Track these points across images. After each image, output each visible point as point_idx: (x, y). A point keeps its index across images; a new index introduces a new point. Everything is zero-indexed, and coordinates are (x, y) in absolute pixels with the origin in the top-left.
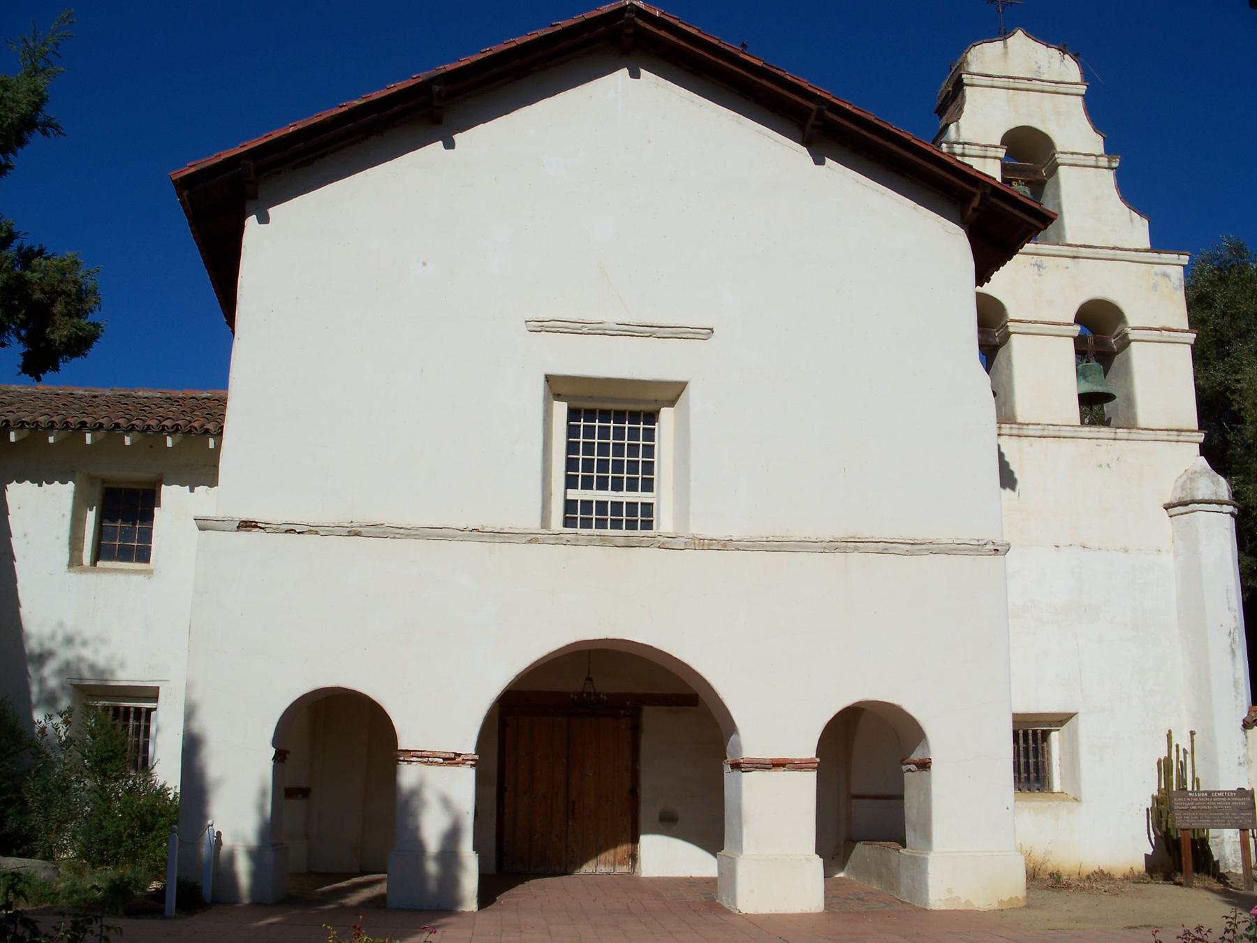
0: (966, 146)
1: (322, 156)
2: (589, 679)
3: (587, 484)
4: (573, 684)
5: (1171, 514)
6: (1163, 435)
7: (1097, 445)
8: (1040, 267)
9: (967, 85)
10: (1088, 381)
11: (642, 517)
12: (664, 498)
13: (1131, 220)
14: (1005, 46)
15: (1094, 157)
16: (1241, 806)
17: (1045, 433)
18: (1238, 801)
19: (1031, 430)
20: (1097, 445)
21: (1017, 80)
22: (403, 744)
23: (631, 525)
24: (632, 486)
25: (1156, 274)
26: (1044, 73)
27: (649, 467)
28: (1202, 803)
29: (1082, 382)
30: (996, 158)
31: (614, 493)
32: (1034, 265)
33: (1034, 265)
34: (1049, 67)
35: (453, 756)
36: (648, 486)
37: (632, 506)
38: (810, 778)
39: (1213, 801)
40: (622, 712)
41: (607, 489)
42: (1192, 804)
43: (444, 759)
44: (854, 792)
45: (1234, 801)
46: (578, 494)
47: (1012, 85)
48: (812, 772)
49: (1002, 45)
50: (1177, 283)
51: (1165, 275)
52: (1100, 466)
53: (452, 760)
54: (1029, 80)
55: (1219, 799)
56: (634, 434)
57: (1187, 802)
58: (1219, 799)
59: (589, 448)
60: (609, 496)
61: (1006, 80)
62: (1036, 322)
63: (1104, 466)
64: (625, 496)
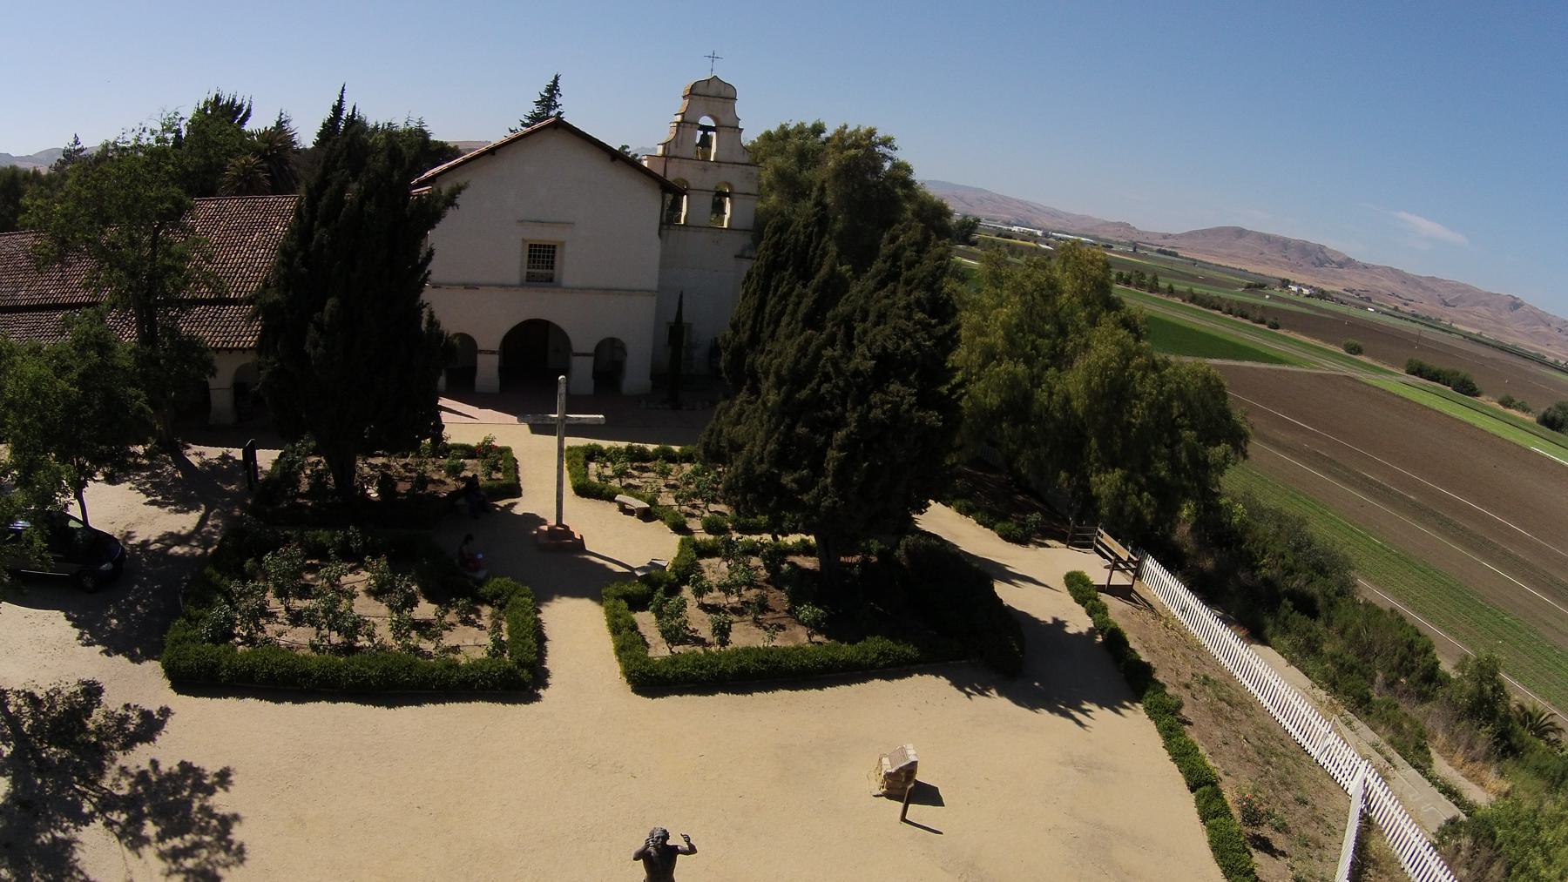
3: (534, 268)
11: (551, 280)
12: (556, 271)
22: (479, 348)
27: (552, 262)
36: (552, 268)
56: (549, 252)
59: (535, 256)
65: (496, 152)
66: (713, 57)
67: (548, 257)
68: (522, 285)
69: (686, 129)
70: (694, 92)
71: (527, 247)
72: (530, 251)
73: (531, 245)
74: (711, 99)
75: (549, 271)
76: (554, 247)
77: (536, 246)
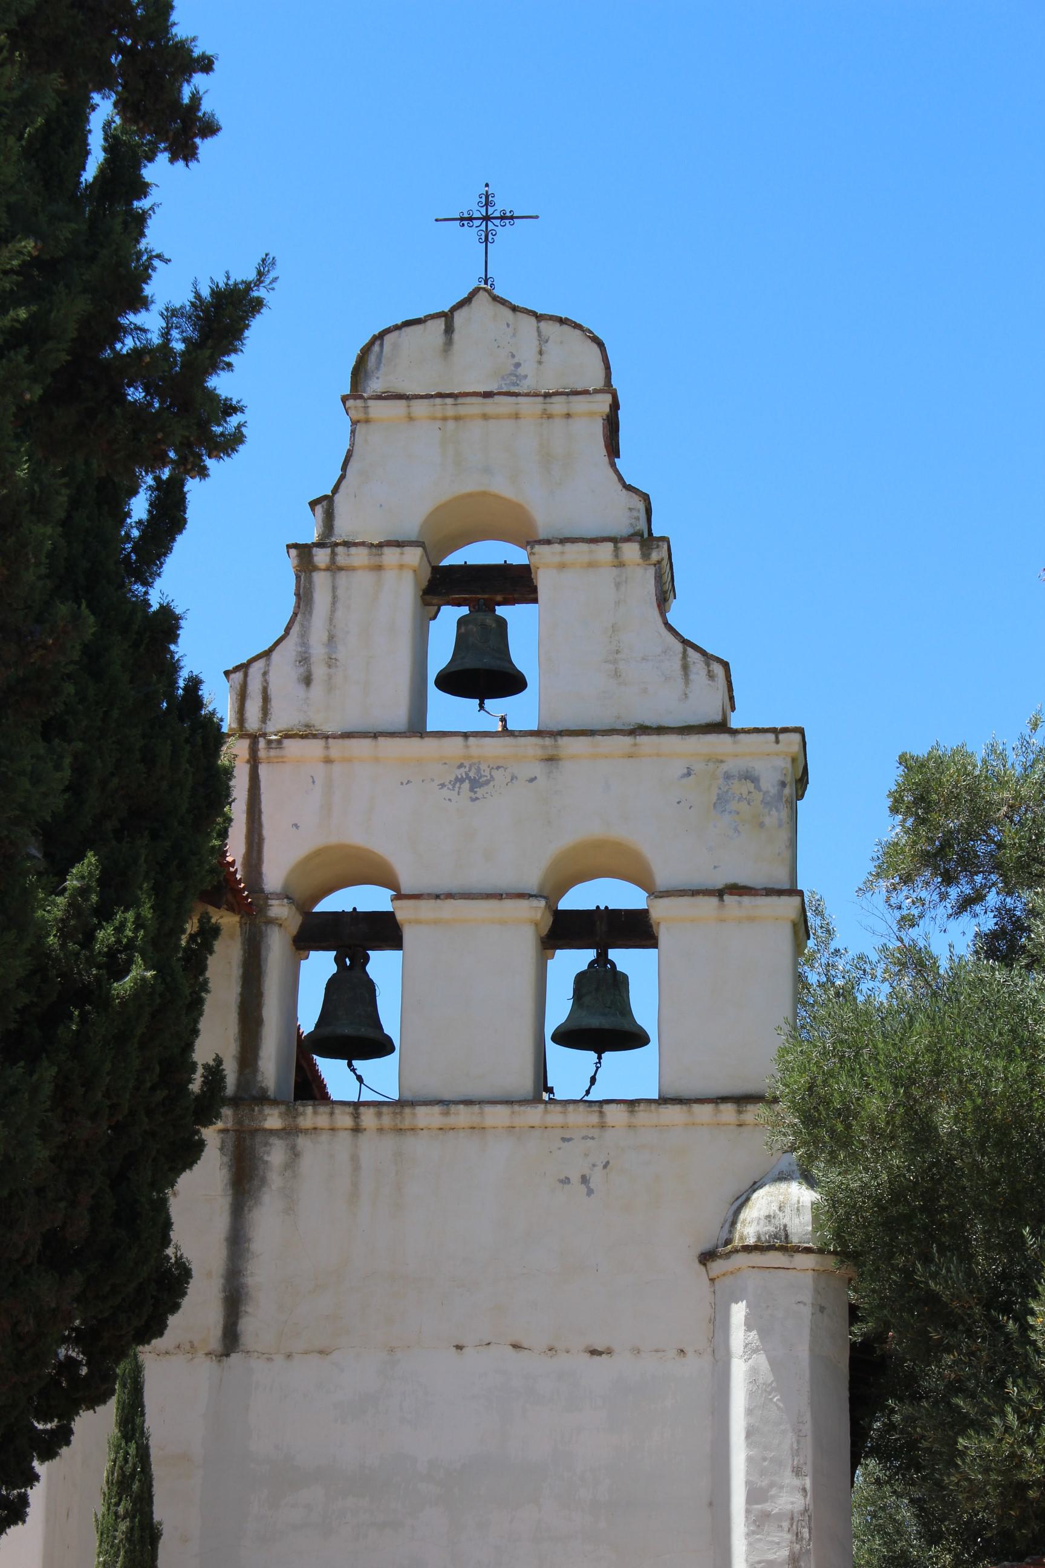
0: (340, 550)
5: (713, 1275)
6: (704, 1112)
7: (564, 1140)
13: (685, 667)
14: (449, 330)
15: (610, 546)
17: (451, 1121)
20: (564, 1140)
21: (460, 400)
25: (728, 776)
26: (526, 377)
30: (401, 567)
32: (461, 780)
33: (461, 780)
34: (540, 363)
47: (450, 411)
49: (443, 327)
50: (774, 791)
51: (749, 777)
52: (566, 1181)
54: (488, 395)
61: (438, 401)
62: (450, 896)
63: (575, 1179)
69: (342, 578)
70: (375, 385)
74: (474, 406)
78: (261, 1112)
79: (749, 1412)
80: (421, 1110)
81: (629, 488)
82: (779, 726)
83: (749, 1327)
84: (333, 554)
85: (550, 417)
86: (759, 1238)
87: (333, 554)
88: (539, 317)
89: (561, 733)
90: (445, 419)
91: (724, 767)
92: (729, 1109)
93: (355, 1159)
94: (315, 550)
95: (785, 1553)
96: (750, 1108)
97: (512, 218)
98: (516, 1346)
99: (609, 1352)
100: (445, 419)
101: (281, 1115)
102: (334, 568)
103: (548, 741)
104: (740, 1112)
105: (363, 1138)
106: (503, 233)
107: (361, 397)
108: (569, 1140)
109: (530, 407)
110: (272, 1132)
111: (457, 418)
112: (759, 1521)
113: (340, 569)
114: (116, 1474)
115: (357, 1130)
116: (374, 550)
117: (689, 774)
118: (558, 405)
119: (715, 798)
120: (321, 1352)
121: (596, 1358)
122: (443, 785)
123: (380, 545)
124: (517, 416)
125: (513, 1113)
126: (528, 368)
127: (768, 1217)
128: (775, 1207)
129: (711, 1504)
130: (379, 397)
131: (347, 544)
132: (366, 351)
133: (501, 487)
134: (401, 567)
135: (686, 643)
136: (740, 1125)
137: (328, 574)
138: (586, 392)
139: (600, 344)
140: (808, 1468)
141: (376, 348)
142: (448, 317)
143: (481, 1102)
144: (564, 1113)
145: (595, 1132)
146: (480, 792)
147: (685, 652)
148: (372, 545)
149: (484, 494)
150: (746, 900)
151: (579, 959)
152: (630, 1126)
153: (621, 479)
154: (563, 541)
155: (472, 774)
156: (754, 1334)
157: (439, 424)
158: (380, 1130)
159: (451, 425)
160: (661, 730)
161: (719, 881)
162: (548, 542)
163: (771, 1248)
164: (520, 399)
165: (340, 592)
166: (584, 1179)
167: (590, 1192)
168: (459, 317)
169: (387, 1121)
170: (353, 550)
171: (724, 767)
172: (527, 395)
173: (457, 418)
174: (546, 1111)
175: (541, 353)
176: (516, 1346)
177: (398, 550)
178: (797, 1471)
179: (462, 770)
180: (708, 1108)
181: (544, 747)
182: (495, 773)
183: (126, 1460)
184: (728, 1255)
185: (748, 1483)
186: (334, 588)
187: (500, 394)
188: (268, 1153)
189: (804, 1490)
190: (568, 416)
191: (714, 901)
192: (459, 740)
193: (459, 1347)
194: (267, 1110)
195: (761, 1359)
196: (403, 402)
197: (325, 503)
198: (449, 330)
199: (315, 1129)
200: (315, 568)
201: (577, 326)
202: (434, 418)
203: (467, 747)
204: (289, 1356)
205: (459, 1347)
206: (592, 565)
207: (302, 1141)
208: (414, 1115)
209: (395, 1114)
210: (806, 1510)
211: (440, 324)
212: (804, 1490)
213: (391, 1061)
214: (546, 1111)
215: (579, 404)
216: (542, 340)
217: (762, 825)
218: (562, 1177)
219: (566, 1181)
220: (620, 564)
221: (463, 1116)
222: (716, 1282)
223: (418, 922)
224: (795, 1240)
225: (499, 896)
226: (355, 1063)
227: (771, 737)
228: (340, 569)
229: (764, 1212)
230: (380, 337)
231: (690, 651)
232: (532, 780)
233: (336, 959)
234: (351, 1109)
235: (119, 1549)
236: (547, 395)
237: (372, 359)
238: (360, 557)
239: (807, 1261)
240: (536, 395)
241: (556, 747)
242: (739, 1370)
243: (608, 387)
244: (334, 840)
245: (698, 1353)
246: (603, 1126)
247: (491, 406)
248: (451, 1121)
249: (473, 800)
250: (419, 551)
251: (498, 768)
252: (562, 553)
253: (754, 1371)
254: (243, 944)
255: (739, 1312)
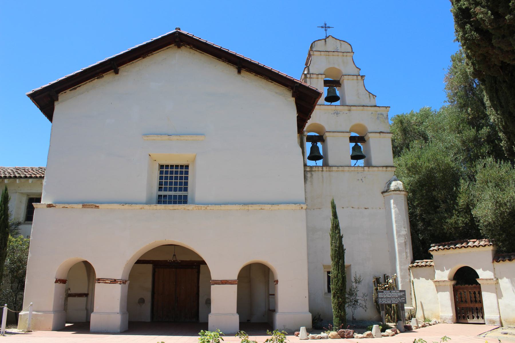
0: (311, 75)
1: (79, 86)
2: (174, 255)
3: (166, 190)
4: (169, 257)
7: (358, 173)
8: (337, 114)
9: (312, 55)
10: (355, 151)
12: (189, 193)
13: (370, 96)
14: (325, 41)
15: (356, 76)
16: (401, 296)
17: (339, 169)
18: (400, 294)
19: (334, 169)
20: (358, 173)
21: (329, 52)
22: (98, 277)
23: (180, 203)
24: (180, 190)
25: (378, 114)
28: (388, 295)
29: (354, 152)
31: (174, 192)
32: (335, 113)
35: (113, 280)
36: (186, 189)
37: (180, 196)
38: (235, 287)
39: (392, 294)
40: (194, 267)
41: (167, 191)
42: (385, 295)
43: (111, 281)
44: (270, 293)
45: (398, 294)
46: (163, 193)
48: (236, 285)
49: (324, 41)
51: (382, 114)
52: (359, 180)
53: (114, 281)
54: (333, 52)
55: (394, 293)
56: (181, 173)
57: (383, 294)
58: (394, 293)
59: (166, 178)
60: (172, 193)
61: (325, 52)
62: (335, 132)
63: (360, 179)
64: (178, 193)
65: (122, 69)
66: (326, 27)
67: (181, 178)
68: (149, 202)
70: (314, 49)
71: (157, 167)
72: (161, 172)
73: (162, 167)
74: (331, 53)
75: (182, 193)
76: (187, 167)
77: (167, 166)
78: (306, 167)
79: (395, 218)
80: (333, 168)
81: (357, 68)
82: (387, 106)
83: (394, 204)
84: (310, 76)
85: (343, 56)
86: (394, 189)
87: (310, 76)
88: (340, 41)
89: (352, 106)
90: (326, 55)
91: (378, 113)
92: (385, 168)
93: (322, 176)
94: (307, 75)
95: (404, 241)
96: (388, 168)
97: (330, 27)
98: (352, 208)
99: (368, 208)
100: (326, 55)
101: (309, 168)
102: (310, 78)
103: (349, 107)
104: (386, 169)
105: (324, 172)
106: (328, 29)
107: (312, 51)
108: (358, 173)
109: (340, 54)
110: (308, 171)
111: (328, 55)
112: (399, 236)
113: (311, 78)
114: (334, 225)
115: (322, 171)
116: (317, 75)
117: (372, 114)
118: (345, 54)
119: (376, 117)
120: (319, 209)
121: (366, 209)
122: (332, 114)
123: (318, 74)
124: (338, 55)
125: (349, 168)
126: (339, 48)
127: (395, 186)
128: (396, 184)
129: (387, 234)
130: (316, 51)
131: (312, 74)
132: (312, 44)
133: (336, 66)
134: (322, 78)
135: (369, 92)
136: (386, 171)
137: (309, 79)
138: (349, 52)
139: (350, 45)
140: (406, 227)
141: (314, 43)
142: (325, 39)
143: (344, 166)
144: (358, 168)
145: (363, 172)
146: (338, 115)
147: (369, 94)
148: (317, 74)
149: (334, 68)
150: (384, 134)
151: (353, 144)
152: (368, 171)
153: (356, 66)
154: (348, 75)
155: (336, 112)
156: (395, 205)
157: (325, 56)
158: (326, 171)
159: (327, 56)
160: (367, 106)
161: (379, 131)
162: (346, 75)
163: (397, 190)
164: (339, 53)
165: (311, 82)
166: (362, 180)
167: (363, 182)
168: (327, 40)
169: (328, 169)
170: (314, 75)
171: (378, 113)
172: (340, 52)
173: (328, 55)
174: (355, 168)
175: (341, 46)
176: (352, 208)
177: (321, 75)
178: (404, 228)
179: (335, 111)
180: (381, 168)
181: (348, 108)
182: (340, 112)
183: (336, 223)
184: (389, 192)
185: (396, 230)
186: (310, 81)
187: (335, 52)
188: (307, 175)
189: (406, 231)
190: (346, 56)
191: (379, 134)
192: (335, 106)
193: (343, 208)
194: (307, 167)
195: (397, 209)
196: (320, 52)
197: (308, 67)
198: (325, 41)
199: (315, 171)
200: (307, 78)
201: (346, 42)
202: (325, 55)
203: (336, 107)
204: (314, 209)
205: (343, 208)
206: (353, 79)
207: (313, 173)
208: (332, 168)
209: (329, 168)
210: (406, 234)
211: (324, 40)
212: (406, 231)
213: (321, 161)
214: (355, 168)
215: (348, 54)
216: (341, 44)
217: (385, 122)
218: (358, 179)
219: (359, 180)
220: (357, 80)
221: (341, 169)
222: (385, 197)
223: (330, 136)
224: (400, 189)
225: (344, 132)
226: (316, 161)
227: (385, 108)
228: (311, 78)
229: (394, 185)
230: (314, 42)
231: (370, 94)
232: (347, 113)
233: (312, 143)
234: (321, 167)
235: (337, 240)
236: (343, 52)
237: (313, 45)
238: (315, 76)
239: (404, 193)
240: (342, 52)
241: (350, 108)
242: (393, 211)
243: (352, 52)
244: (314, 122)
245: (383, 208)
246: (364, 171)
247: (334, 53)
248: (339, 169)
249: (337, 116)
250: (325, 75)
251: (341, 111)
252: (348, 77)
253: (395, 211)
254: (300, 139)
255: (392, 201)
